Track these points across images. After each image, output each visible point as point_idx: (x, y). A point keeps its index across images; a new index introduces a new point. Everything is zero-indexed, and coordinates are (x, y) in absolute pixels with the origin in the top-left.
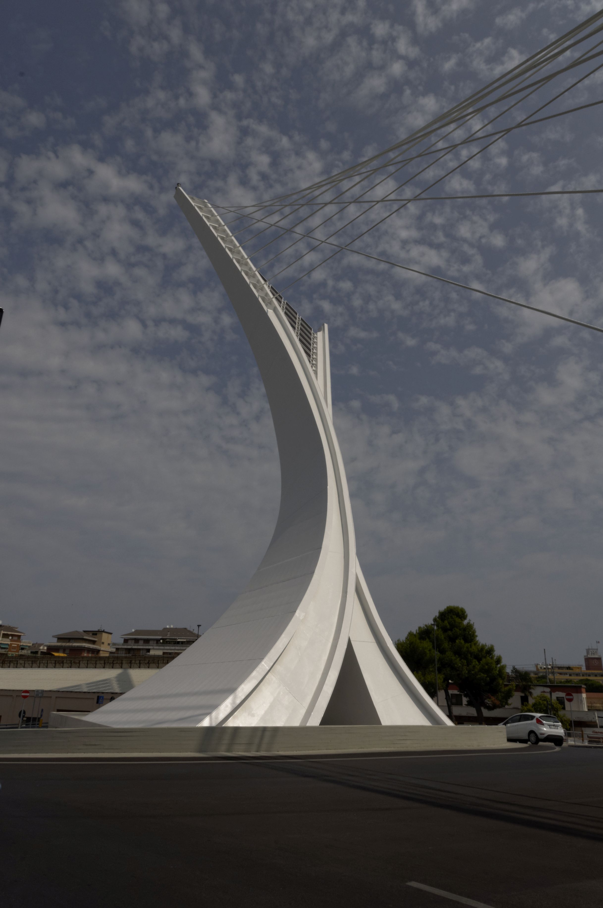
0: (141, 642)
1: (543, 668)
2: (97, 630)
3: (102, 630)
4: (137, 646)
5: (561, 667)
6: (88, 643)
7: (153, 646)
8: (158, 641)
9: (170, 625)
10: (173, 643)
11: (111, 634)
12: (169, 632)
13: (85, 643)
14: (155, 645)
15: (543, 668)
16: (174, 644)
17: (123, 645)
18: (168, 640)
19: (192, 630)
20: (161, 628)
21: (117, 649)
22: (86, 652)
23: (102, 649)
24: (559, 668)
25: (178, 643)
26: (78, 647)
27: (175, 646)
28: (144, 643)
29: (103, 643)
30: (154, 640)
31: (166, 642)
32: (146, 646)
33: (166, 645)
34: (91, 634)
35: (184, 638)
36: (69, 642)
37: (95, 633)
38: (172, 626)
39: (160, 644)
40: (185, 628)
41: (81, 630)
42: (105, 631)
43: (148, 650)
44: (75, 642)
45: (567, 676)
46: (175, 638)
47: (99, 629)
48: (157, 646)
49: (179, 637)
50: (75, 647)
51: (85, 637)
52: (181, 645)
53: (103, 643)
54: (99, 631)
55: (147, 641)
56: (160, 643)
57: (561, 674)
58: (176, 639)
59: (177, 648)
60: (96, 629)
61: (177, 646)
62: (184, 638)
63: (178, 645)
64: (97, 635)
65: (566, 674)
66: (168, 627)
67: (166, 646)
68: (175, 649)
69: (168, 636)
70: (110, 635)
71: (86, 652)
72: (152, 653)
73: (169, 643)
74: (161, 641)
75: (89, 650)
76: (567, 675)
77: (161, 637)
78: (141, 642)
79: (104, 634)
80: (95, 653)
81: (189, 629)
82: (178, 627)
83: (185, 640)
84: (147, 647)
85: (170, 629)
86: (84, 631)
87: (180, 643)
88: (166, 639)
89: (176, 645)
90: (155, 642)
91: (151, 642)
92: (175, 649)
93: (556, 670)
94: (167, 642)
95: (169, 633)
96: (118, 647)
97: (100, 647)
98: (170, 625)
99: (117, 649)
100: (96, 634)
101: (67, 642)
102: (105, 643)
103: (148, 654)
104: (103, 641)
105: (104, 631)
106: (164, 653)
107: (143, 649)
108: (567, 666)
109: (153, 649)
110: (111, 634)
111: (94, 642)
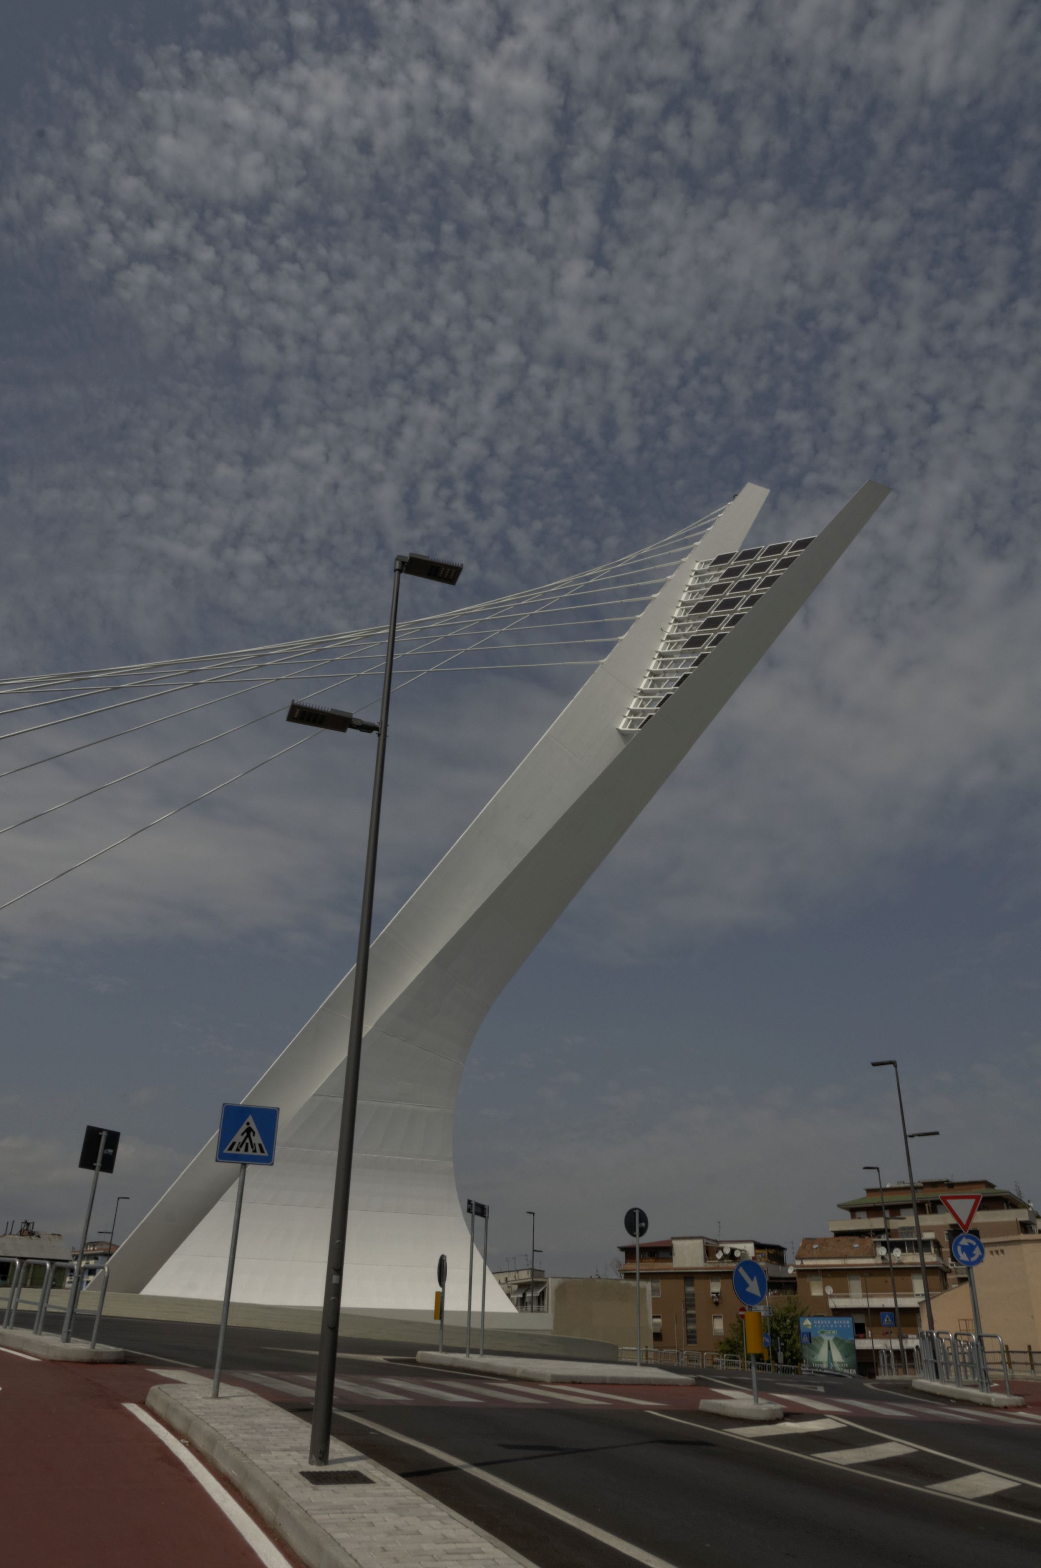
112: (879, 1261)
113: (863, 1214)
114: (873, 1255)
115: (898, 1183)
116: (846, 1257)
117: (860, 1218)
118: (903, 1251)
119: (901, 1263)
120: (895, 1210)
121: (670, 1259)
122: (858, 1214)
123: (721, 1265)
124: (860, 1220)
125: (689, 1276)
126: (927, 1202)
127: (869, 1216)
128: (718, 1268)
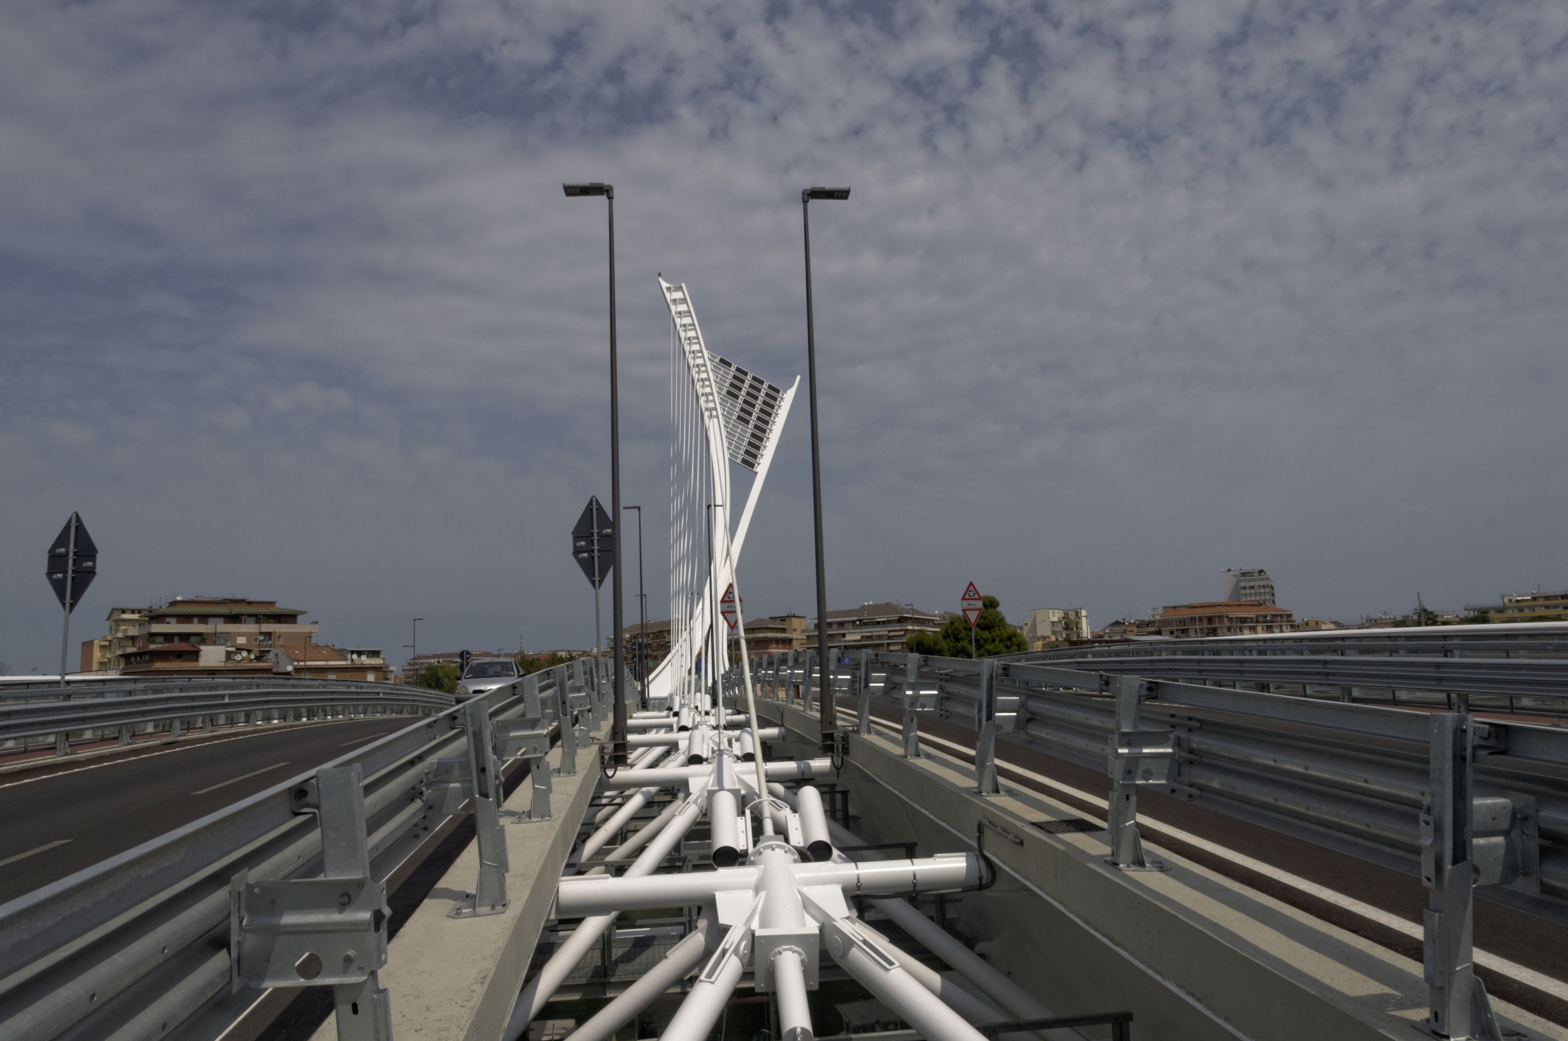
0: (835, 626)
1: (1513, 601)
2: (785, 615)
3: (792, 615)
4: (832, 630)
5: (1550, 596)
6: (777, 632)
7: (848, 629)
8: (854, 622)
9: (868, 602)
10: (871, 624)
11: (804, 617)
12: (865, 610)
13: (773, 632)
14: (851, 628)
15: (1513, 601)
16: (874, 624)
17: (813, 631)
18: (865, 621)
19: (898, 604)
20: (857, 607)
21: (808, 637)
22: (774, 642)
23: (795, 637)
24: (1547, 598)
25: (878, 623)
26: (763, 638)
27: (874, 628)
28: (838, 627)
29: (795, 630)
30: (849, 622)
31: (863, 624)
32: (839, 630)
33: (864, 627)
34: (779, 621)
35: (885, 616)
36: (753, 633)
37: (783, 619)
38: (871, 603)
39: (856, 627)
40: (888, 604)
41: (766, 616)
42: (796, 615)
43: (844, 635)
44: (760, 633)
45: (1559, 609)
46: (874, 617)
47: (788, 613)
48: (853, 629)
49: (878, 615)
50: (759, 638)
51: (769, 626)
52: (882, 625)
53: (795, 630)
54: (788, 617)
55: (841, 624)
56: (857, 625)
57: (1547, 607)
58: (875, 619)
59: (877, 629)
60: (784, 614)
61: (877, 627)
62: (885, 616)
63: (878, 626)
64: (788, 621)
65: (1557, 606)
66: (866, 604)
67: (864, 628)
68: (875, 631)
69: (866, 617)
70: (802, 620)
71: (774, 642)
72: (848, 638)
73: (867, 625)
74: (858, 623)
75: (778, 641)
76: (1559, 608)
77: (856, 618)
78: (835, 626)
79: (793, 619)
80: (787, 643)
81: (895, 604)
82: (878, 604)
83: (885, 619)
84: (842, 632)
85: (869, 606)
86: (771, 618)
87: (881, 623)
88: (863, 620)
89: (875, 626)
90: (851, 624)
91: (847, 625)
92: (875, 631)
93: (1541, 602)
94: (864, 623)
95: (866, 612)
96: (808, 634)
97: (792, 634)
98: (868, 602)
99: (808, 637)
100: (785, 620)
101: (751, 634)
102: (797, 630)
103: (844, 639)
104: (794, 627)
105: (794, 616)
106: (862, 637)
107: (837, 634)
108: (1563, 593)
109: (849, 633)
110: (804, 617)
111: (783, 630)
112: (349, 662)
113: (173, 620)
114: (346, 660)
115: (196, 597)
116: (328, 660)
117: (169, 623)
118: (368, 657)
119: (363, 664)
120: (204, 618)
121: (197, 660)
122: (168, 620)
123: (239, 664)
124: (169, 625)
125: (212, 672)
126: (243, 615)
127: (178, 622)
128: (237, 667)
